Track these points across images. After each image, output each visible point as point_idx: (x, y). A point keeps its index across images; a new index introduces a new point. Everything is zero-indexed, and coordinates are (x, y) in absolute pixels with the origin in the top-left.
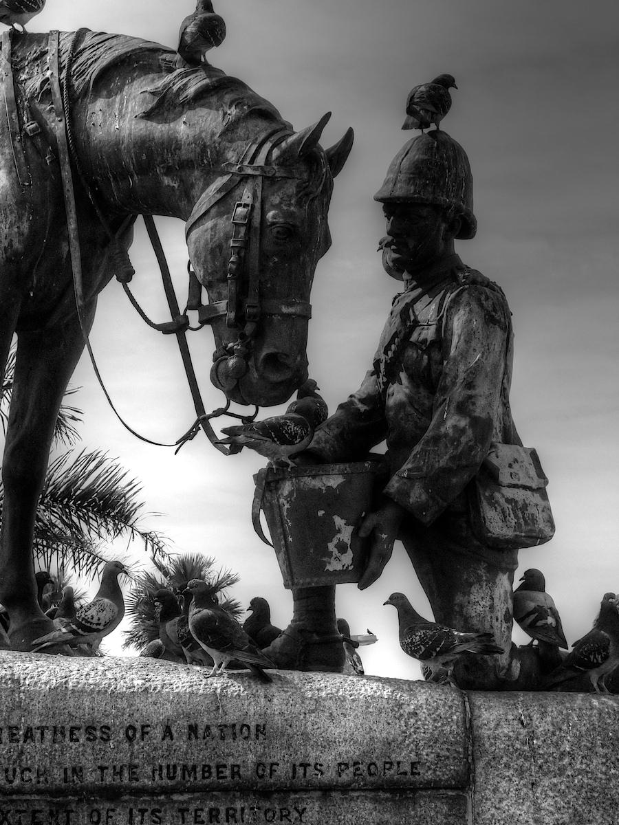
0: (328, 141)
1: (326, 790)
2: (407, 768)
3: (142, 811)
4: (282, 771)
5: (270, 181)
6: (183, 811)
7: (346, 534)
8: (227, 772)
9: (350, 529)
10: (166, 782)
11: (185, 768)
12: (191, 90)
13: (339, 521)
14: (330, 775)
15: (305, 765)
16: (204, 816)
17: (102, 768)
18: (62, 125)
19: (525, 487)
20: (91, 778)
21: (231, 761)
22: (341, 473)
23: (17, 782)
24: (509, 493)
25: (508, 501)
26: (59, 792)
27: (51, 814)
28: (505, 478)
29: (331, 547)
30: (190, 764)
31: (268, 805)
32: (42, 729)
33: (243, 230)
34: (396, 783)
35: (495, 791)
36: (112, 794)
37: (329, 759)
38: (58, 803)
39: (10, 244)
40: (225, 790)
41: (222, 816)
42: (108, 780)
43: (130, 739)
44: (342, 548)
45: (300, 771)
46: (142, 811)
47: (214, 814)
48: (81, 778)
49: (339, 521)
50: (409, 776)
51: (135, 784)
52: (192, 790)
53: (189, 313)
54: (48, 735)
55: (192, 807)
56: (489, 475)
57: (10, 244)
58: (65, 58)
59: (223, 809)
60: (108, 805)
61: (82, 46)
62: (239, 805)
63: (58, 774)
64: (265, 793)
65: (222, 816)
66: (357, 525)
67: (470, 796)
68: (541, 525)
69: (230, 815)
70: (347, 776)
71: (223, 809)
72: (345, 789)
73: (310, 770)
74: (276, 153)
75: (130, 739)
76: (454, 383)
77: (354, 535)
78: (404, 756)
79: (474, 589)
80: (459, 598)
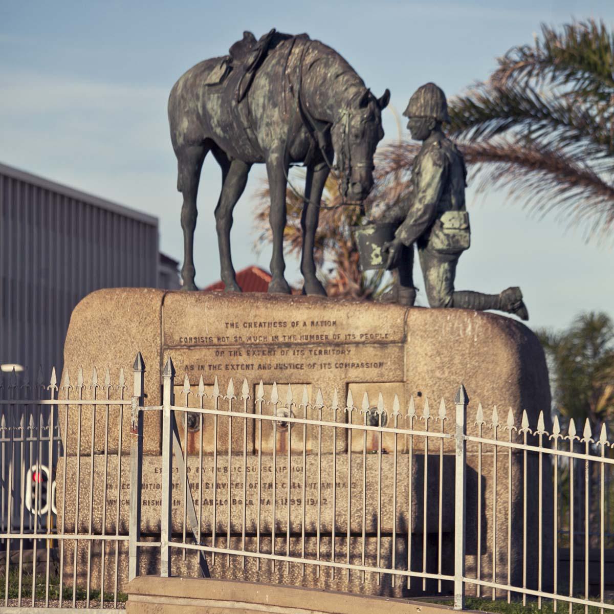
1: (357, 344)
3: (298, 351)
8: (324, 338)
10: (305, 341)
15: (349, 335)
16: (317, 352)
20: (281, 339)
21: (325, 334)
23: (258, 341)
36: (288, 345)
46: (298, 351)
51: (295, 342)
54: (267, 325)
55: (314, 350)
60: (287, 349)
62: (329, 348)
64: (338, 345)
65: (323, 353)
69: (326, 352)
73: (351, 337)
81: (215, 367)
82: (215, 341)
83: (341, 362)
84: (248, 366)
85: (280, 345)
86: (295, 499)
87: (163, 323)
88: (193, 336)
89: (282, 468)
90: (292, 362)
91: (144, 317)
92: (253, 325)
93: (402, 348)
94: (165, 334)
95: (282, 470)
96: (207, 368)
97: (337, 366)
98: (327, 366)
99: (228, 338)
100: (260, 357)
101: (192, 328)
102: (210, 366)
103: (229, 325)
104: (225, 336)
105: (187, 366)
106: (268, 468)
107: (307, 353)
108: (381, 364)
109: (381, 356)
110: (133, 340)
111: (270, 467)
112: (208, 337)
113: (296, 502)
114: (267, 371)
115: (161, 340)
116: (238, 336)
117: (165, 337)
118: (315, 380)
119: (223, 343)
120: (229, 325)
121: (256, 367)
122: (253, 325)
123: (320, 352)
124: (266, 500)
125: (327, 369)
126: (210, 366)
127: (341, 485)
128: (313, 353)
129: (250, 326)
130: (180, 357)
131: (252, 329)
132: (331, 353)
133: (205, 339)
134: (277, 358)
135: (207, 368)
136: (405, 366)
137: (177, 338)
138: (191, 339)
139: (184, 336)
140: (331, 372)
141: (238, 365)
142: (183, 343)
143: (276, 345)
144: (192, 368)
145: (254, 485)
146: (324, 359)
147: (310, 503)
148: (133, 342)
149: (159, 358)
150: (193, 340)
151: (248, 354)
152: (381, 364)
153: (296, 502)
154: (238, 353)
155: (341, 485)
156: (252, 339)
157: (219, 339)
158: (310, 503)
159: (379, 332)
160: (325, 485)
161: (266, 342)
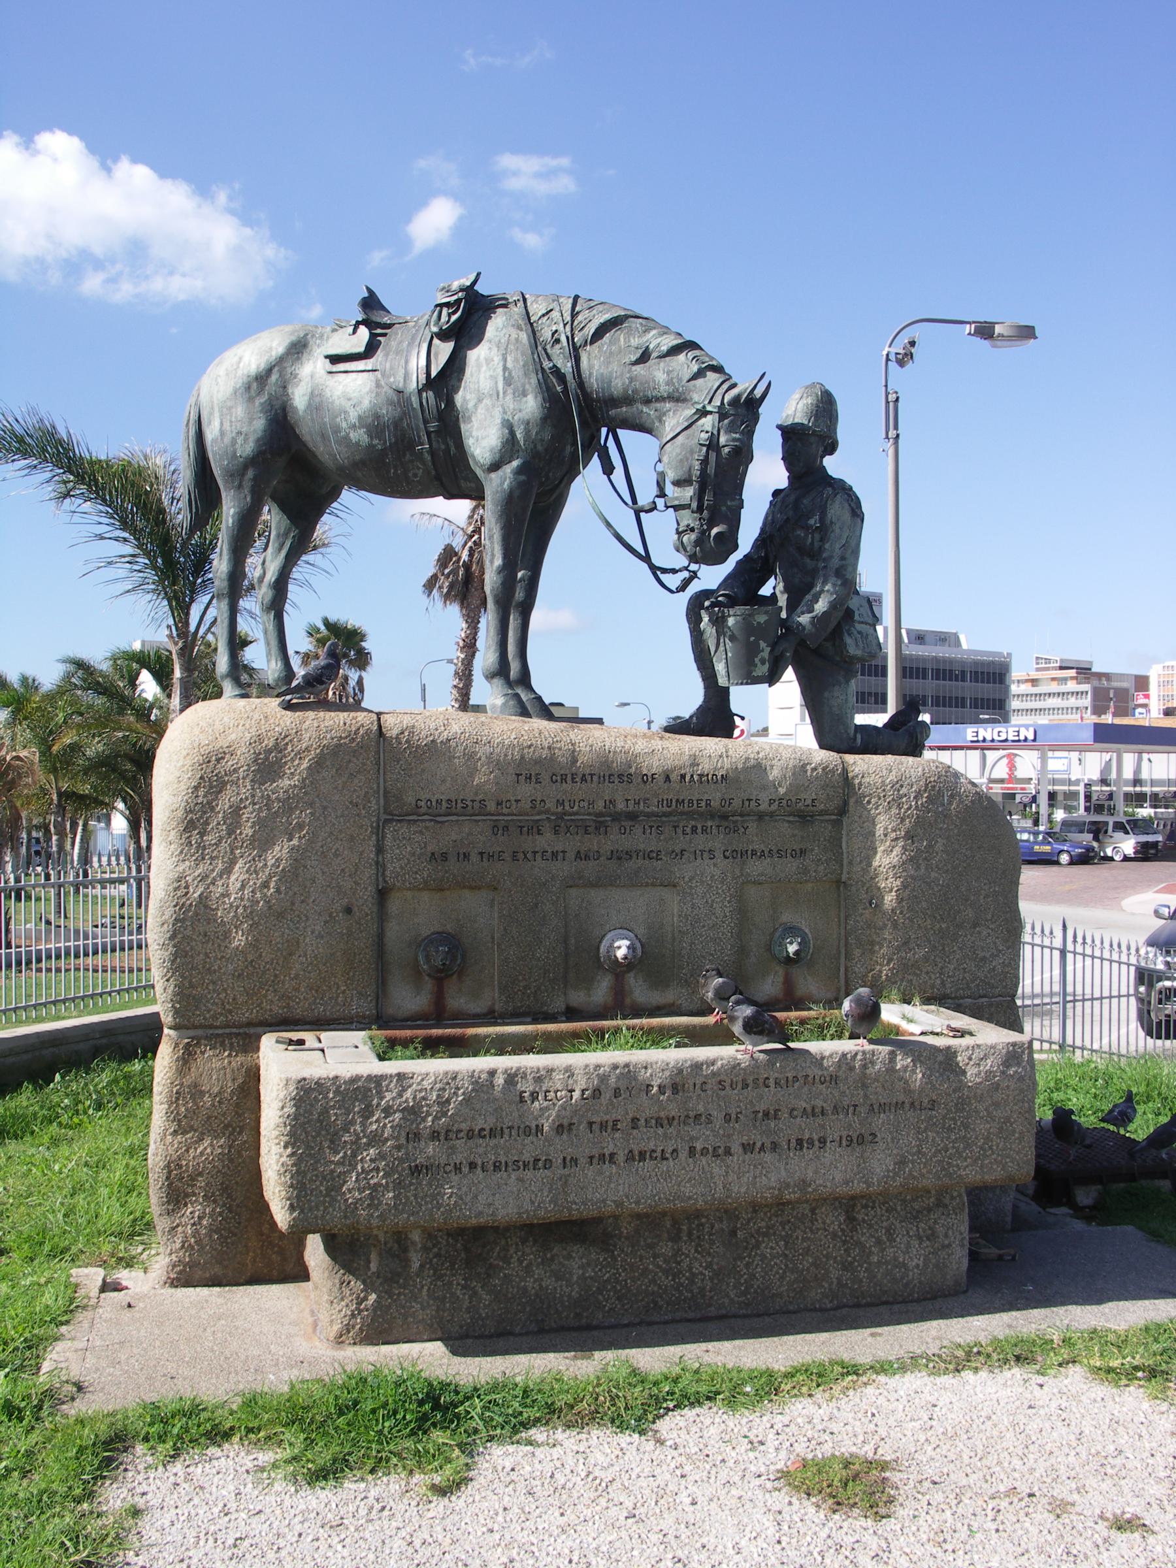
0: (758, 393)
1: (761, 816)
2: (809, 802)
3: (651, 827)
4: (737, 803)
5: (722, 415)
6: (675, 827)
7: (766, 654)
8: (703, 804)
9: (769, 649)
10: (666, 809)
11: (677, 801)
12: (664, 348)
13: (762, 644)
14: (764, 807)
15: (749, 800)
16: (688, 830)
17: (627, 800)
18: (569, 365)
19: (866, 623)
20: (621, 806)
21: (706, 797)
22: (766, 613)
23: (576, 808)
24: (859, 627)
25: (860, 633)
26: (601, 814)
27: (596, 828)
28: (856, 617)
29: (757, 660)
30: (681, 798)
31: (726, 824)
32: (592, 775)
33: (705, 449)
34: (803, 811)
35: (860, 817)
36: (633, 816)
37: (764, 797)
38: (601, 822)
39: (535, 446)
40: (701, 815)
41: (699, 830)
42: (631, 808)
43: (645, 782)
44: (763, 662)
45: (747, 803)
46: (651, 827)
47: (694, 830)
48: (614, 806)
49: (762, 644)
50: (811, 808)
51: (647, 810)
52: (682, 813)
53: (657, 500)
54: (595, 778)
55: (681, 825)
56: (849, 614)
57: (535, 446)
58: (568, 318)
59: (699, 827)
60: (630, 823)
61: (577, 309)
62: (709, 824)
63: (601, 804)
64: (725, 817)
65: (699, 830)
66: (773, 646)
67: (845, 820)
68: (875, 647)
69: (704, 830)
70: (774, 807)
71: (699, 827)
72: (772, 815)
73: (753, 803)
74: (727, 398)
75: (645, 782)
76: (831, 557)
77: (771, 651)
78: (808, 796)
79: (836, 688)
80: (826, 694)
81: (491, 856)
82: (491, 806)
83: (734, 847)
84: (555, 855)
85: (617, 817)
86: (816, 1137)
87: (381, 771)
88: (444, 797)
89: (790, 1079)
90: (642, 846)
91: (347, 757)
92: (569, 778)
93: (838, 824)
94: (386, 792)
95: (790, 1083)
96: (474, 858)
97: (727, 854)
98: (706, 855)
99: (517, 801)
100: (578, 838)
101: (443, 781)
102: (481, 854)
103: (522, 778)
104: (512, 799)
105: (433, 854)
106: (761, 1081)
107: (667, 830)
108: (803, 852)
109: (802, 837)
110: (325, 804)
111: (767, 1078)
112: (478, 799)
113: (816, 1143)
114: (591, 863)
115: (378, 803)
116: (539, 799)
117: (385, 796)
118: (686, 879)
119: (505, 811)
120: (522, 778)
121: (571, 855)
122: (569, 778)
123: (694, 830)
124: (759, 1145)
125: (707, 861)
126: (481, 854)
127: (907, 1106)
128: (680, 831)
129: (564, 778)
130: (418, 837)
131: (567, 786)
132: (714, 831)
133: (469, 803)
134: (614, 840)
135: (474, 858)
136: (845, 856)
137: (410, 799)
138: (439, 802)
139: (424, 796)
140: (715, 865)
141: (535, 853)
142: (423, 810)
143: (610, 815)
144: (444, 857)
145: (734, 1116)
146: (700, 841)
147: (844, 1143)
148: (325, 808)
149: (374, 838)
150: (444, 804)
151: (556, 832)
152: (803, 852)
153: (816, 1143)
154: (535, 830)
155: (907, 1106)
156: (567, 804)
157: (499, 804)
158: (844, 1143)
159: (802, 796)
160: (876, 1107)
161: (591, 810)
